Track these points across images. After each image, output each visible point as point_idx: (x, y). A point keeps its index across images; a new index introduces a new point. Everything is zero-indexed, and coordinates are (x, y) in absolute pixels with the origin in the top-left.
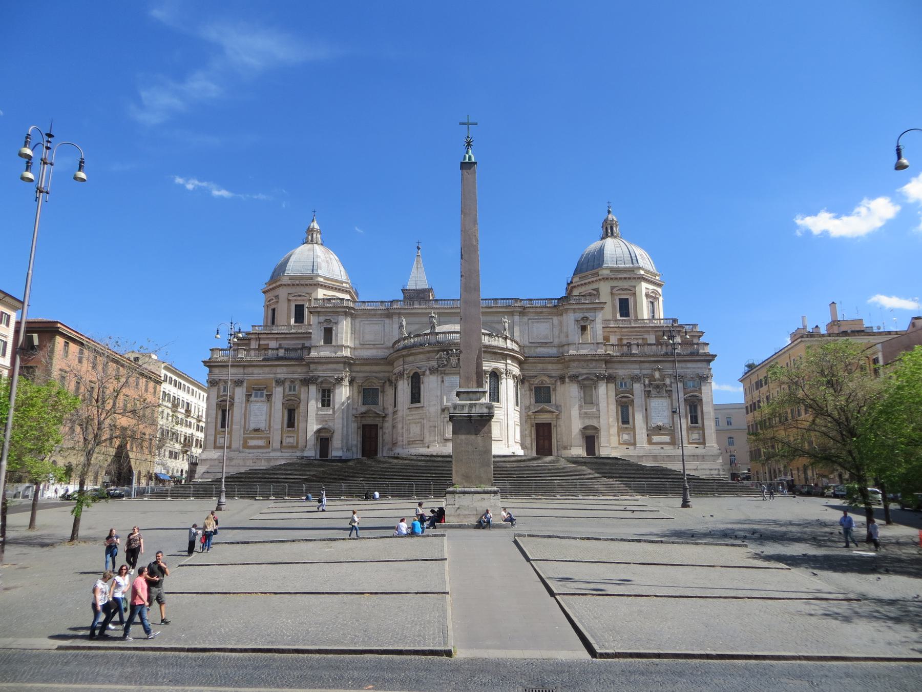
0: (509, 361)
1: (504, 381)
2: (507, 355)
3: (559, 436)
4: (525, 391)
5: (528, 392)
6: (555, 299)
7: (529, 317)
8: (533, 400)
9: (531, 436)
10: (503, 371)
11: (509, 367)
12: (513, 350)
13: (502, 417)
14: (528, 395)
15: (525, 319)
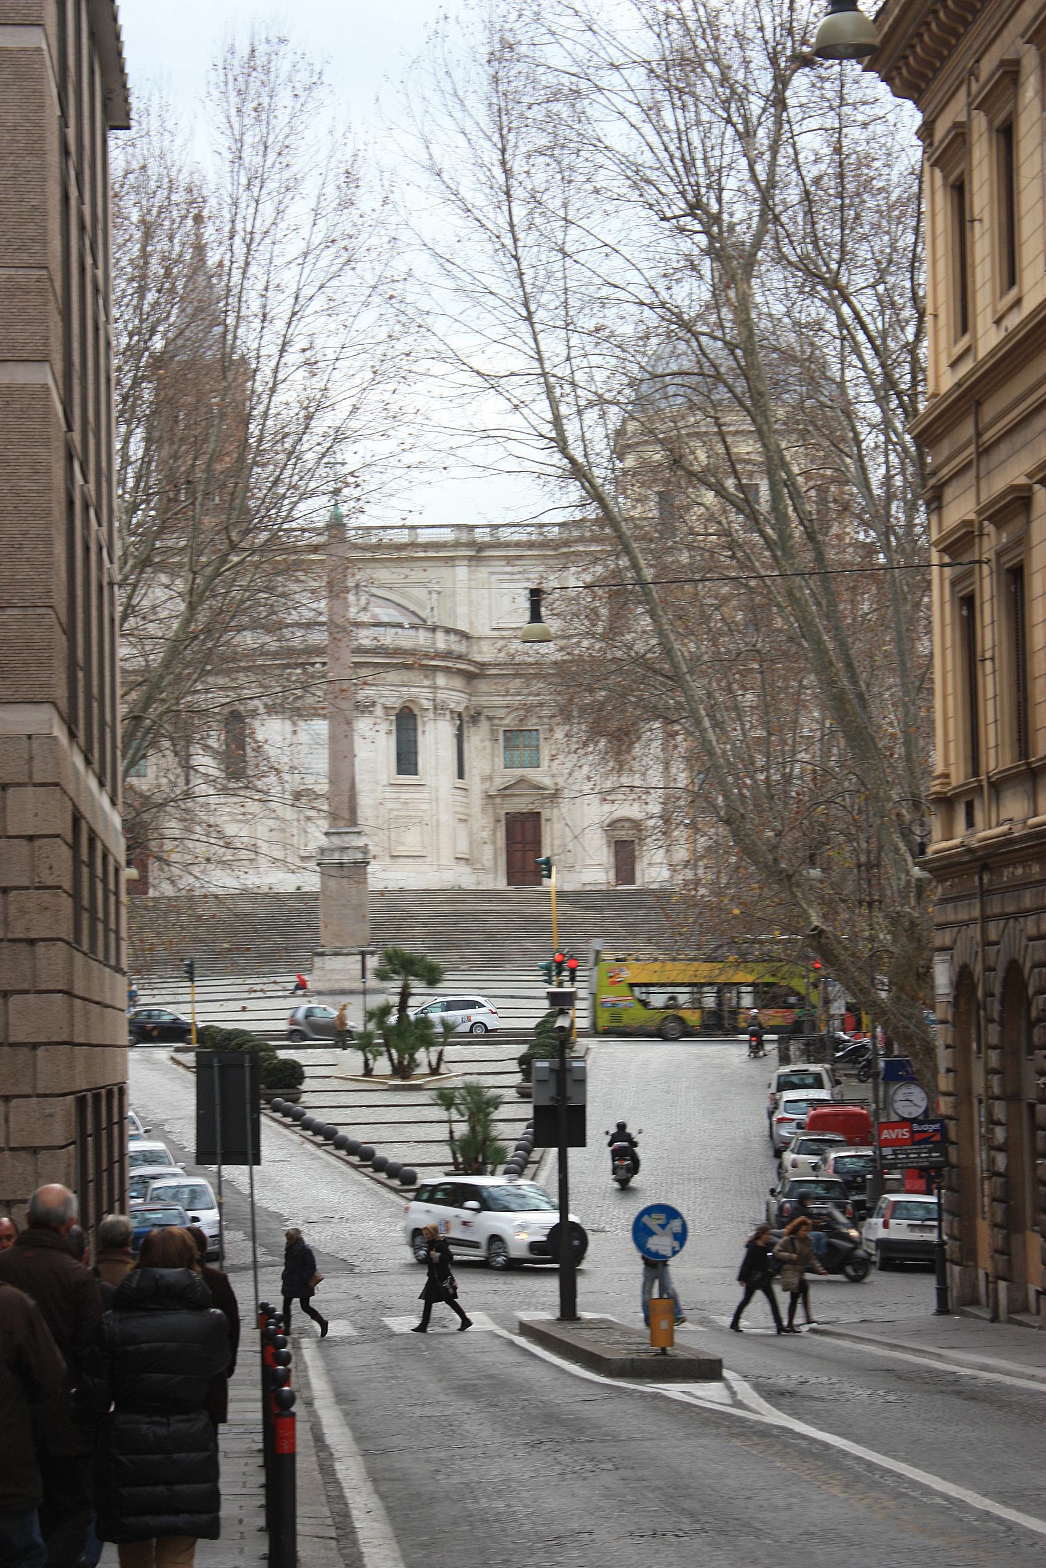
0: (441, 680)
1: (430, 727)
2: (436, 668)
3: (557, 842)
4: (482, 741)
5: (488, 744)
6: (554, 525)
7: (491, 569)
8: (500, 761)
9: (494, 843)
10: (426, 704)
11: (441, 696)
12: (448, 655)
13: (425, 806)
14: (488, 751)
15: (483, 573)
